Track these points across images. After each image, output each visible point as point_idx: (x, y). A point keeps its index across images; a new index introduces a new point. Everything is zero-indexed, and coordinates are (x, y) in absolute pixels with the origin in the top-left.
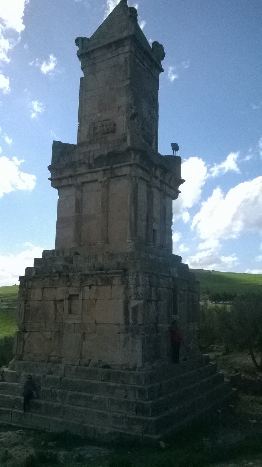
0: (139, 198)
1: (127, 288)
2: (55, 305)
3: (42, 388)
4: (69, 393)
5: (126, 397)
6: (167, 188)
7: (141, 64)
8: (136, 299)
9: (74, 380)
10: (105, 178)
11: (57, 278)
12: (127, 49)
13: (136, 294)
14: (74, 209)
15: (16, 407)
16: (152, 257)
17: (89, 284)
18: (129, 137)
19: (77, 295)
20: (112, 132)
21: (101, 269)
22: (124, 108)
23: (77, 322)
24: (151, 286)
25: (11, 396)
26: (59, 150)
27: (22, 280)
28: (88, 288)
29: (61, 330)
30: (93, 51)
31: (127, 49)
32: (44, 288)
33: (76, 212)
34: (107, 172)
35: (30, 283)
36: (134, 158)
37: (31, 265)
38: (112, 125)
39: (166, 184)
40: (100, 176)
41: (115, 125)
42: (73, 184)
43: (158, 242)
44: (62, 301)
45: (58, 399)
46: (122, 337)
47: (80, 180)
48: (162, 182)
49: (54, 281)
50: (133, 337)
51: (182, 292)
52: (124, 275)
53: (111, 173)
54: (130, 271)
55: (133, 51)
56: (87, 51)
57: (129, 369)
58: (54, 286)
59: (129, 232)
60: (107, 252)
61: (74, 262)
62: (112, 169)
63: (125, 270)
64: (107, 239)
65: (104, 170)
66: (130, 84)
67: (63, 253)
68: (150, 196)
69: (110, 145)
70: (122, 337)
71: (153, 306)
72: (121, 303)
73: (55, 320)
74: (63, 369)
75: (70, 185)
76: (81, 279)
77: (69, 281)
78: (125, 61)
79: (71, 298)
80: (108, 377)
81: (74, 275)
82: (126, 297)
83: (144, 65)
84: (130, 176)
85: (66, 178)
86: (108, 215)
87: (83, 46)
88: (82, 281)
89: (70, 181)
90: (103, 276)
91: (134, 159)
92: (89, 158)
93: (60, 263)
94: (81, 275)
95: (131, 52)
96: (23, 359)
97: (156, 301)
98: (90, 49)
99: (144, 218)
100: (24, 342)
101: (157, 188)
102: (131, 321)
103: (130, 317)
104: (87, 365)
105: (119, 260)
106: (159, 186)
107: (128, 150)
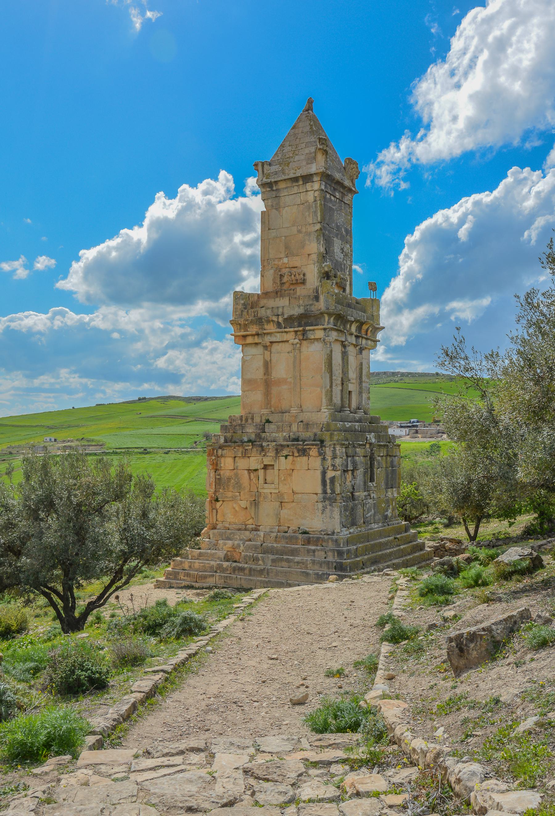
0: (334, 362)
1: (324, 459)
2: (249, 474)
3: (243, 553)
4: (271, 557)
5: (325, 558)
6: (364, 341)
7: (333, 198)
8: (333, 470)
9: (275, 545)
10: (297, 341)
12: (316, 186)
13: (333, 466)
14: (262, 371)
15: (218, 571)
16: (348, 425)
18: (322, 298)
19: (273, 465)
20: (301, 283)
21: (297, 440)
22: (314, 257)
23: (273, 491)
24: (347, 456)
25: (212, 563)
26: (242, 302)
28: (284, 458)
30: (276, 182)
31: (316, 186)
32: (235, 457)
33: (265, 374)
34: (298, 333)
35: (220, 451)
36: (328, 322)
38: (302, 276)
39: (362, 337)
40: (290, 337)
41: (304, 275)
42: (260, 343)
43: (354, 405)
44: (256, 470)
45: (260, 562)
46: (320, 505)
47: (268, 339)
48: (357, 337)
50: (330, 505)
51: (379, 458)
52: (322, 447)
53: (303, 335)
54: (327, 443)
55: (323, 187)
56: (269, 180)
57: (329, 535)
58: (245, 455)
59: (324, 400)
60: (302, 422)
62: (304, 330)
63: (322, 441)
64: (301, 407)
65: (296, 332)
66: (321, 229)
67: (252, 419)
68: (344, 354)
69: (301, 302)
70: (320, 505)
71: (349, 476)
72: (318, 474)
74: (262, 536)
75: (256, 344)
76: (277, 450)
77: (263, 450)
78: (315, 201)
79: (265, 467)
80: (308, 542)
81: (268, 445)
82: (324, 468)
83: (335, 197)
84: (324, 340)
85: (253, 335)
86: (300, 380)
87: (263, 171)
89: (257, 340)
90: (299, 446)
91: (329, 323)
92: (278, 315)
93: (251, 431)
94: (276, 445)
95: (322, 190)
96: (218, 527)
97: (353, 471)
98: (273, 180)
99: (339, 382)
100: (217, 512)
101: (352, 344)
102: (329, 491)
103: (328, 487)
104: (286, 532)
105: (315, 430)
106: (354, 343)
107: (322, 314)
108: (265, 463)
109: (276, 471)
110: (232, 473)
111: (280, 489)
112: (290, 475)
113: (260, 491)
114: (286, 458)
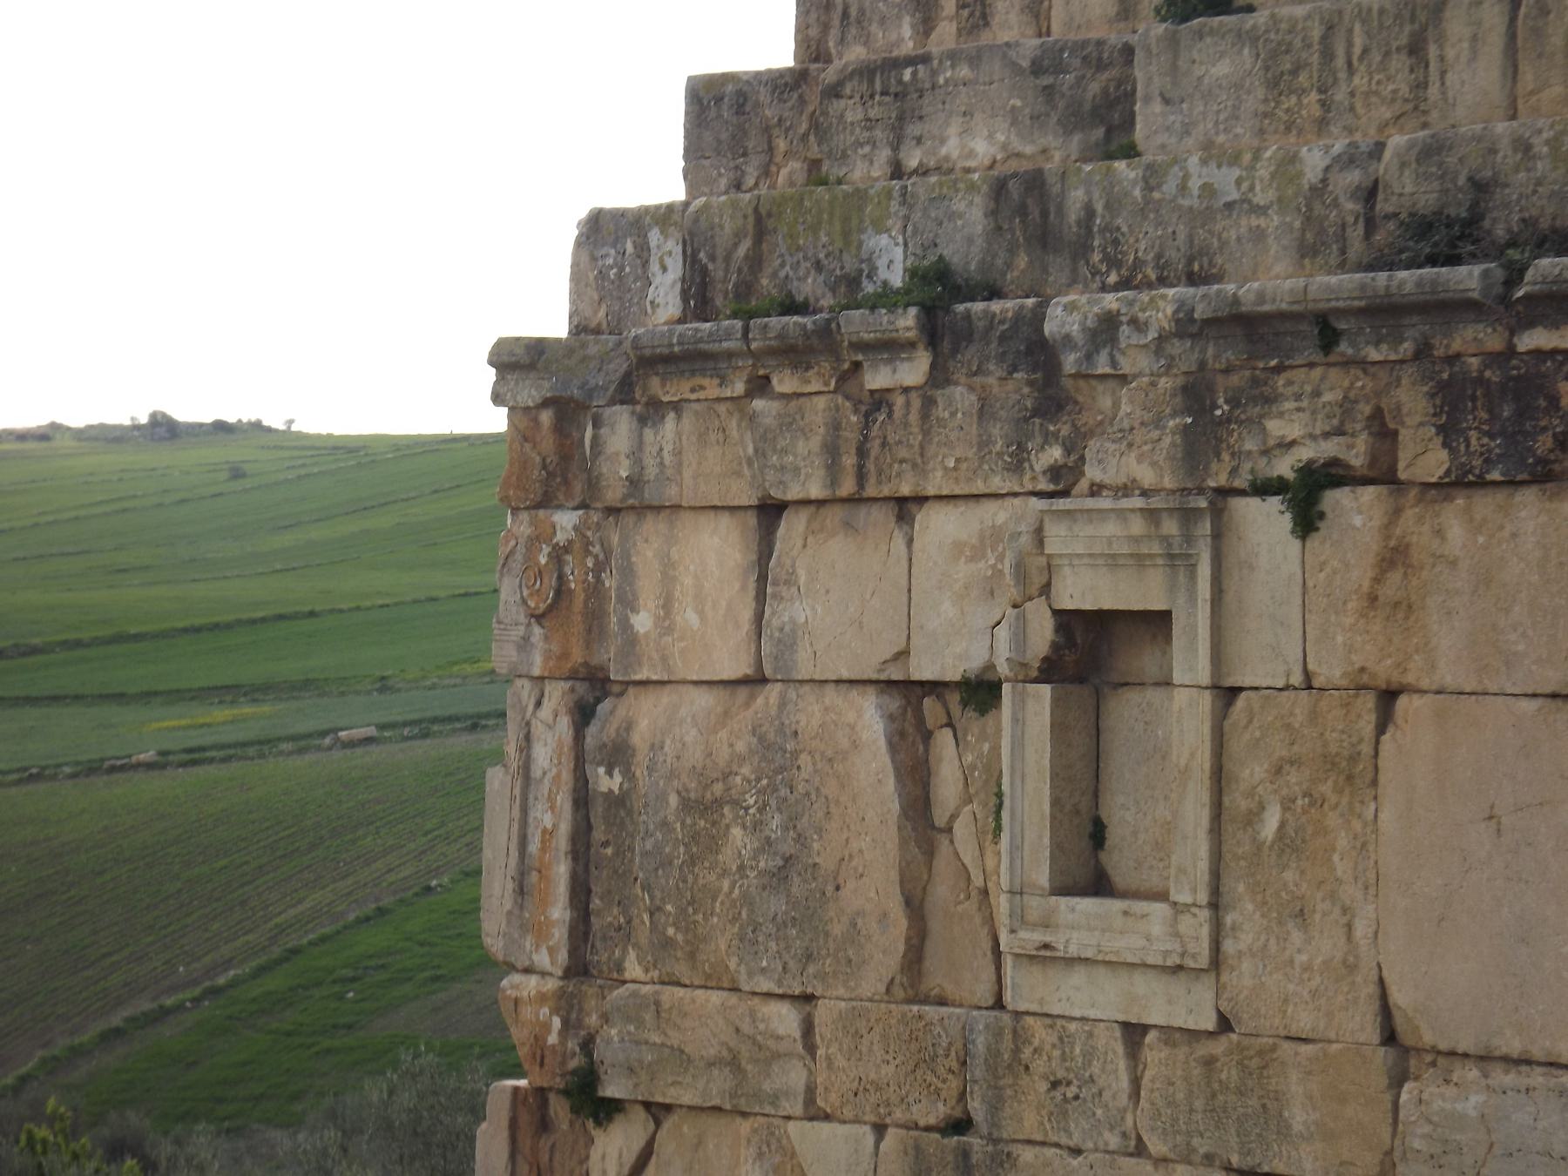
11: (913, 371)
17: (1284, 467)
19: (1158, 622)
21: (1446, 235)
27: (530, 394)
29: (977, 1108)
32: (770, 511)
37: (654, 173)
44: (981, 692)
49: (880, 400)
61: (1149, 121)
73: (914, 958)
76: (1195, 395)
88: (1204, 418)
94: (1186, 326)
108: (1082, 590)
109: (1184, 718)
110: (734, 741)
111: (1242, 976)
112: (1358, 775)
113: (1027, 989)
114: (1306, 522)
